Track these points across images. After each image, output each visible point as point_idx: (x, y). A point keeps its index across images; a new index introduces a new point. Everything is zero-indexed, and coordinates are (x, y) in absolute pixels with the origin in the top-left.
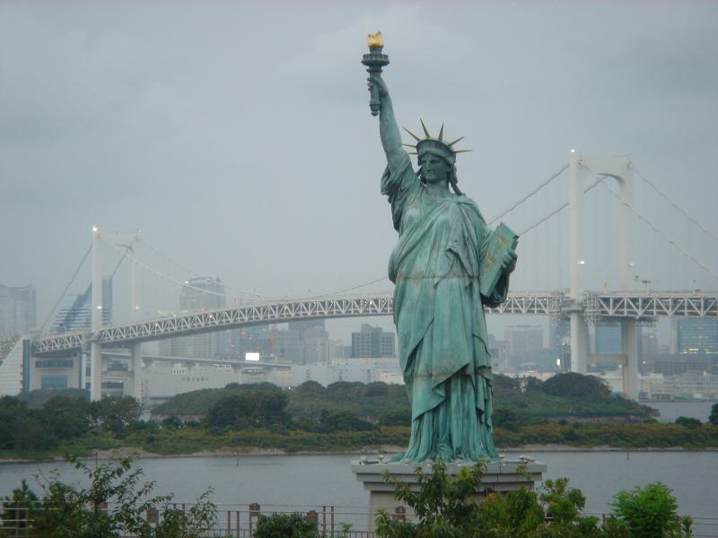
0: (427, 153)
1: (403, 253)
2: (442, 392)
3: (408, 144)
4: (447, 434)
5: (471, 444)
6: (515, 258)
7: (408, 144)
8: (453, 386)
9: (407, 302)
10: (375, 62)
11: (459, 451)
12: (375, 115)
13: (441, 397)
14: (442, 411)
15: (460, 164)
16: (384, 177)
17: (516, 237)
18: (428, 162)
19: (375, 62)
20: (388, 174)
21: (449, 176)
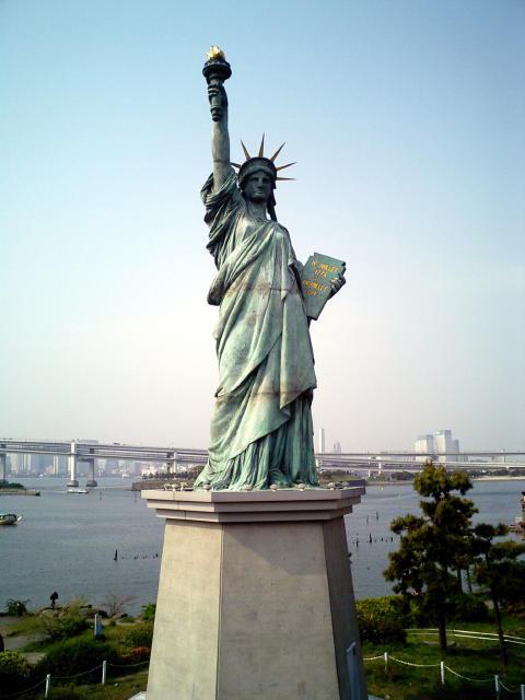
0: (260, 170)
1: (245, 262)
2: (288, 413)
3: (238, 158)
4: (280, 457)
5: (310, 467)
6: (343, 282)
7: (238, 158)
8: (297, 406)
9: (248, 314)
10: (218, 71)
11: (298, 477)
12: (215, 120)
13: (286, 415)
14: (280, 434)
15: (280, 192)
16: (203, 191)
17: (344, 264)
18: (260, 180)
19: (218, 71)
20: (209, 187)
21: (270, 203)
